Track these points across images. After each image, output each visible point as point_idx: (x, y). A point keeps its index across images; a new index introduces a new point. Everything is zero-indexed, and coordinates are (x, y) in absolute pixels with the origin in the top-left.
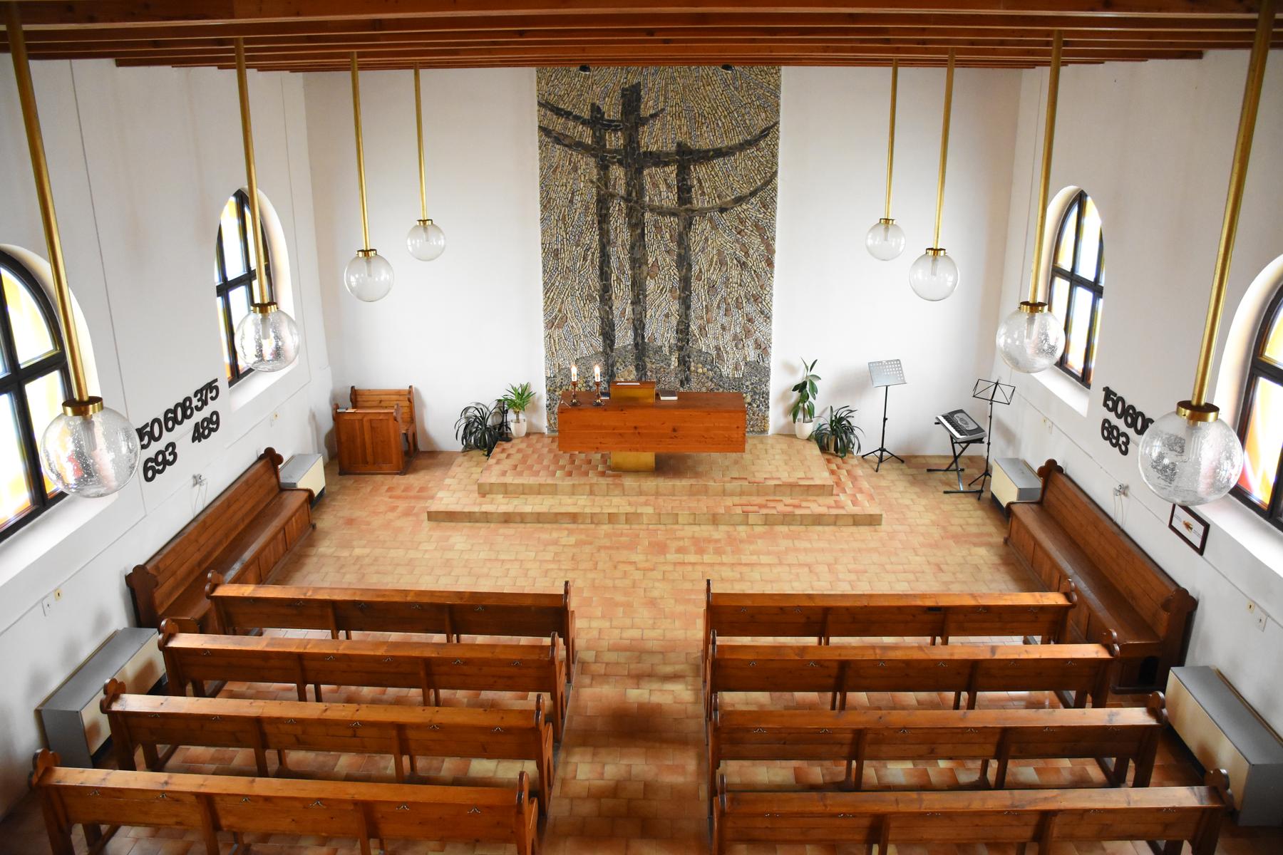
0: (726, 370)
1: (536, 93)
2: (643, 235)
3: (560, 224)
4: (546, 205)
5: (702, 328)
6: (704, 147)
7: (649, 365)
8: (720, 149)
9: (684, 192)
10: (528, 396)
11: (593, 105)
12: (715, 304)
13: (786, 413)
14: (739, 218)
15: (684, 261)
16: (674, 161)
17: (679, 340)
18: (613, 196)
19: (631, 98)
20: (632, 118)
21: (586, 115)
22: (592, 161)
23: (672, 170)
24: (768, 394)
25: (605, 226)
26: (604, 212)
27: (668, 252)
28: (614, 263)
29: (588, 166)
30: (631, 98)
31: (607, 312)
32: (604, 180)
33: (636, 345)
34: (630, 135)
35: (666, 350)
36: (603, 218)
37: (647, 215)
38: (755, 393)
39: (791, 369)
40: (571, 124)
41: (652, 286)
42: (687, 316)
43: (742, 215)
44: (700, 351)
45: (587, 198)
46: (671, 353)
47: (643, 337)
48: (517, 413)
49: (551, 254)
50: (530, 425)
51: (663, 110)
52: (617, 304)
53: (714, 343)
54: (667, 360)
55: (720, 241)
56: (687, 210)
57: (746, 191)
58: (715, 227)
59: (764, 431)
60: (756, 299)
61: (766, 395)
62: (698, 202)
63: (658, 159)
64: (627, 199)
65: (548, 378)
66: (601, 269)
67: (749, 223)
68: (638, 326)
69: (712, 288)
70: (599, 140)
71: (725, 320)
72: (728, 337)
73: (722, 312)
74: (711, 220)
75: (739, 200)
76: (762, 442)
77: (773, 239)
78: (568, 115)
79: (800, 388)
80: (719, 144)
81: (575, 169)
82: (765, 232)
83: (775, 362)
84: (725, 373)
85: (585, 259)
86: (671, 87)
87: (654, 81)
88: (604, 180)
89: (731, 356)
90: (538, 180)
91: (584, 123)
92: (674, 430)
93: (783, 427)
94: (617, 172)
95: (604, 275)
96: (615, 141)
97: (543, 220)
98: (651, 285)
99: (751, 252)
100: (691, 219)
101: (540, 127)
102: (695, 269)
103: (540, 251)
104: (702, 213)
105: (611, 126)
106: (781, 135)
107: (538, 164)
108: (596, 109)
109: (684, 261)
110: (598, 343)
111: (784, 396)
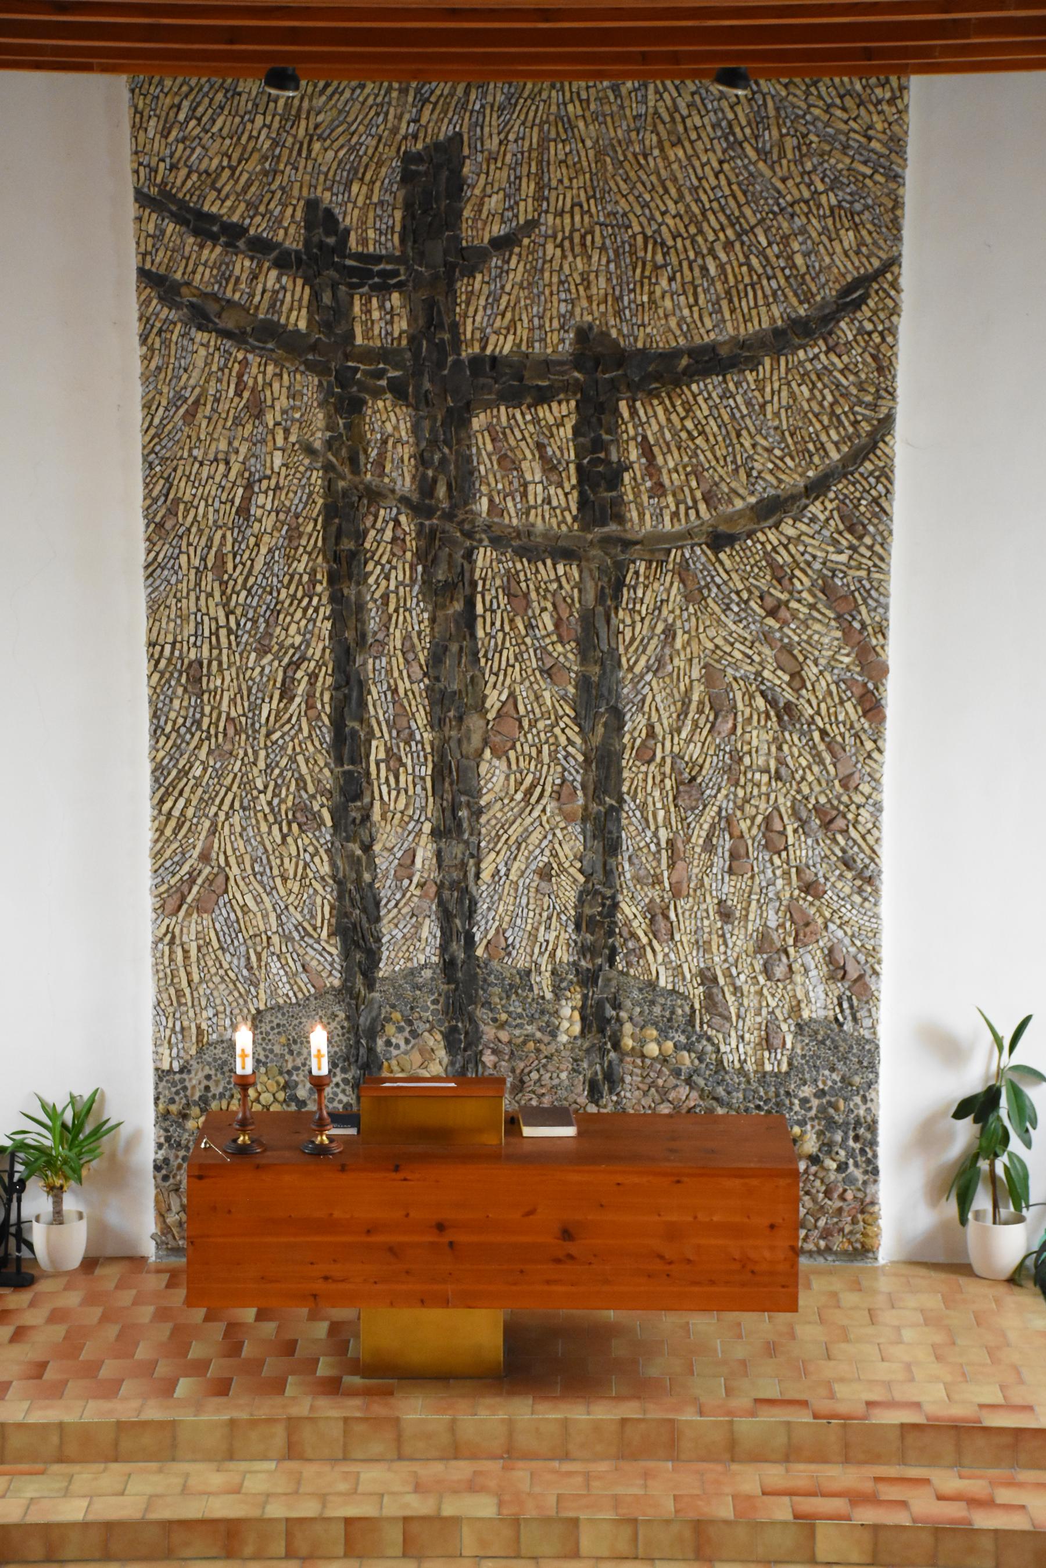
0: (737, 1049)
1: (128, 165)
2: (469, 618)
3: (209, 580)
4: (164, 519)
5: (655, 914)
6: (661, 344)
7: (489, 1032)
8: (712, 348)
9: (598, 484)
10: (98, 1132)
11: (312, 205)
12: (698, 838)
13: (937, 1191)
14: (772, 565)
15: (598, 701)
16: (569, 388)
17: (584, 950)
18: (374, 496)
19: (433, 184)
20: (436, 249)
21: (291, 237)
22: (309, 385)
23: (561, 415)
24: (872, 1127)
25: (350, 591)
26: (348, 545)
27: (548, 673)
28: (378, 705)
29: (295, 399)
30: (433, 184)
31: (355, 863)
32: (347, 447)
33: (448, 966)
34: (430, 305)
35: (543, 983)
36: (345, 566)
37: (484, 557)
38: (831, 1124)
39: (947, 1048)
40: (243, 265)
41: (497, 781)
42: (609, 874)
43: (783, 557)
44: (652, 985)
45: (294, 500)
46: (557, 991)
48: (56, 1192)
49: (179, 675)
50: (99, 1231)
51: (532, 224)
52: (387, 838)
53: (692, 963)
54: (545, 1015)
55: (711, 637)
56: (606, 541)
57: (794, 481)
58: (695, 595)
59: (864, 1251)
60: (828, 819)
61: (865, 1132)
62: (643, 518)
63: (518, 382)
64: (420, 506)
65: (161, 1075)
66: (338, 724)
67: (802, 582)
68: (455, 905)
69: (687, 785)
70: (333, 319)
71: (729, 888)
72: (740, 940)
73: (720, 863)
74: (683, 571)
75: (772, 509)
76: (857, 1286)
77: (881, 630)
78: (232, 234)
79: (979, 1107)
80: (708, 333)
81: (257, 410)
82: (855, 609)
83: (893, 1021)
84: (731, 1059)
85: (287, 693)
86: (556, 151)
87: (504, 129)
88: (347, 447)
89: (751, 1001)
90: (137, 442)
91: (284, 262)
92: (567, 1234)
93: (929, 1239)
94: (389, 422)
95: (347, 744)
96: (381, 321)
97: (152, 568)
98: (494, 776)
99: (811, 671)
100: (621, 567)
101: (144, 275)
102: (635, 725)
103: (144, 666)
104: (657, 549)
105: (370, 275)
106: (907, 300)
107: (137, 390)
108: (320, 219)
109: (598, 701)
110: (326, 960)
111: (926, 1136)
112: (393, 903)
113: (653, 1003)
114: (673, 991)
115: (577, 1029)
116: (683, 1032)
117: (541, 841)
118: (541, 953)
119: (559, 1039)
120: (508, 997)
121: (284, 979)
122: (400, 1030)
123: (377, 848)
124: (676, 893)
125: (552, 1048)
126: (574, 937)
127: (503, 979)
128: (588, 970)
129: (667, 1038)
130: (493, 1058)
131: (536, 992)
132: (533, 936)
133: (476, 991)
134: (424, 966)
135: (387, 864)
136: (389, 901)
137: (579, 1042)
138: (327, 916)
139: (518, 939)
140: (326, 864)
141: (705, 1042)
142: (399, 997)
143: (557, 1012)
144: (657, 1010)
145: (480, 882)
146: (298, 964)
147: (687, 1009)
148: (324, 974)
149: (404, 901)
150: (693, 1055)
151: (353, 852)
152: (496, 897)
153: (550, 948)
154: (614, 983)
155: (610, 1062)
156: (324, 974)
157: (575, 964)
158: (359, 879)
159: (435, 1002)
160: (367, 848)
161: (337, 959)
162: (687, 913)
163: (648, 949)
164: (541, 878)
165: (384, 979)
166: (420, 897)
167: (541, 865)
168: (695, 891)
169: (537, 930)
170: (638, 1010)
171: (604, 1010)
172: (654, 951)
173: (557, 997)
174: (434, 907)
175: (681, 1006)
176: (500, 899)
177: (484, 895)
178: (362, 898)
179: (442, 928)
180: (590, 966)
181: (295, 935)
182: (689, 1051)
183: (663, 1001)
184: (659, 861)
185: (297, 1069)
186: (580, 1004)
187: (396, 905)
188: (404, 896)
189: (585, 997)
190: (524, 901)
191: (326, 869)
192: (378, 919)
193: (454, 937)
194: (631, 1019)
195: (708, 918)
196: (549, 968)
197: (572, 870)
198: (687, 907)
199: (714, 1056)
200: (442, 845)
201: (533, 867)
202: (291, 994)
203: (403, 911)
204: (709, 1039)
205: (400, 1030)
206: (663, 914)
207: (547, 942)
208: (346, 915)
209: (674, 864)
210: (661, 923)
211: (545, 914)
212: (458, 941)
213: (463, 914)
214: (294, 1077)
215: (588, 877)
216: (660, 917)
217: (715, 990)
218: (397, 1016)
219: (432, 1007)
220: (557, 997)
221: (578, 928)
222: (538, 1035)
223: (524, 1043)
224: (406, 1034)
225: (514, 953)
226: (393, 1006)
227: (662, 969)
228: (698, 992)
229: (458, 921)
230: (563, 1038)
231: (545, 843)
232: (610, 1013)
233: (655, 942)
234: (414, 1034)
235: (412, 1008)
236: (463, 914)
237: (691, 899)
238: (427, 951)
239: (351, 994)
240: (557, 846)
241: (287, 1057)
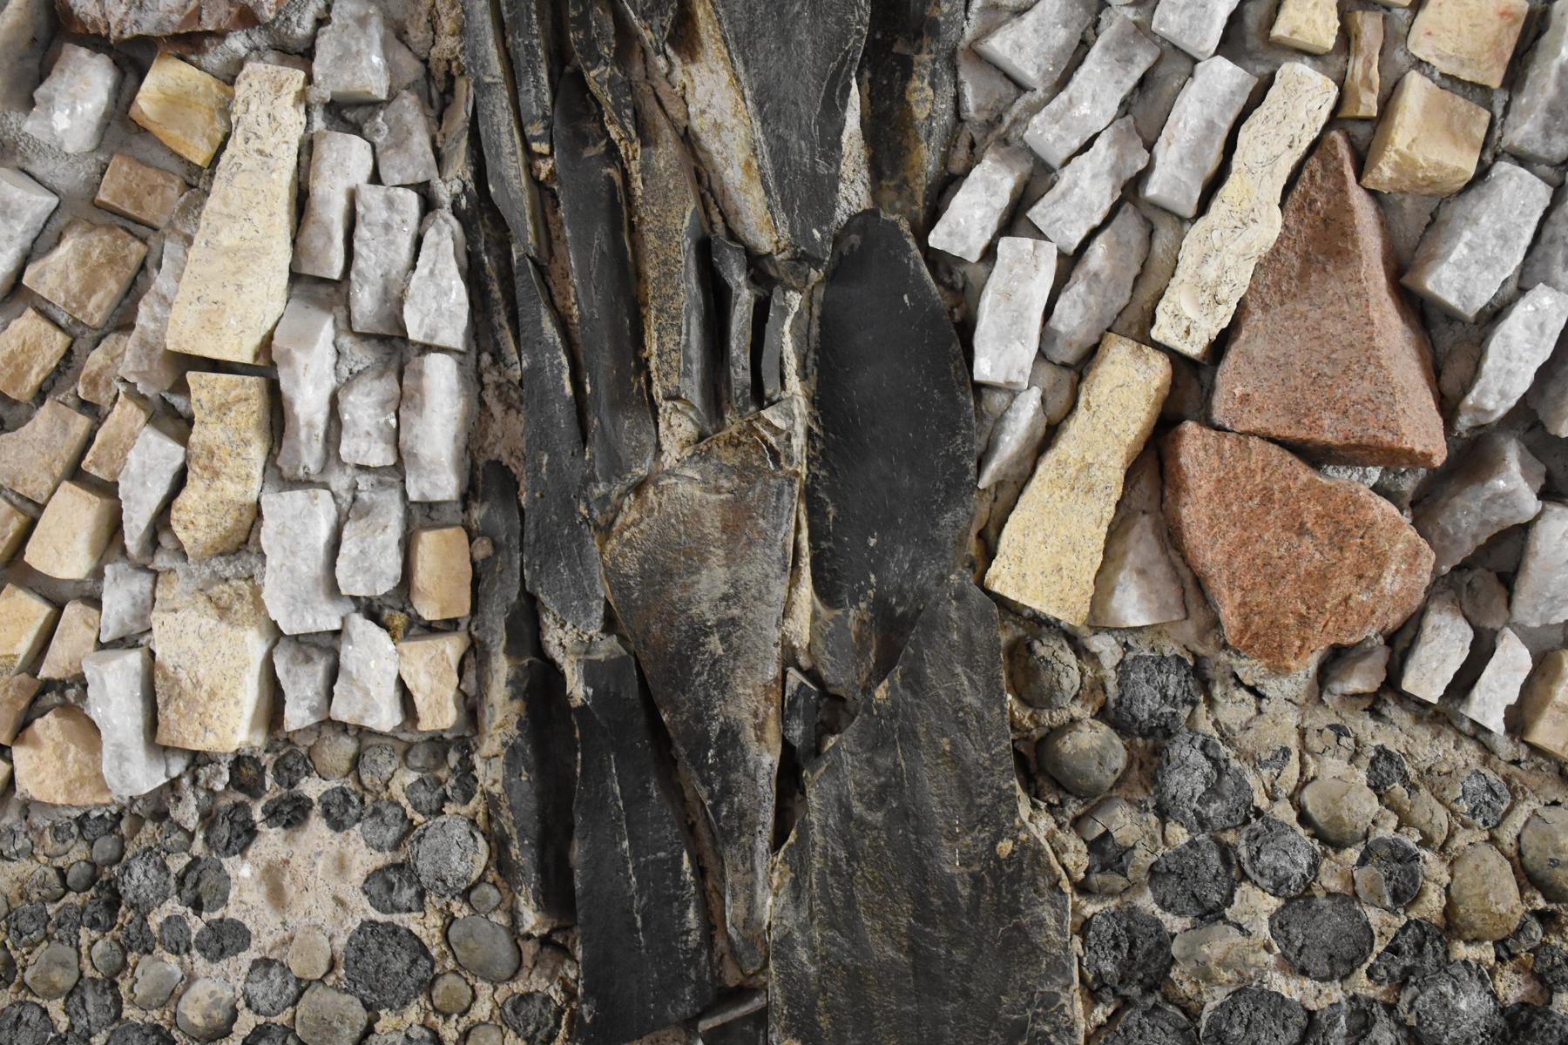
47: (898, 410)
134: (262, 788)
179: (481, 216)
193: (673, 343)
229: (713, 94)
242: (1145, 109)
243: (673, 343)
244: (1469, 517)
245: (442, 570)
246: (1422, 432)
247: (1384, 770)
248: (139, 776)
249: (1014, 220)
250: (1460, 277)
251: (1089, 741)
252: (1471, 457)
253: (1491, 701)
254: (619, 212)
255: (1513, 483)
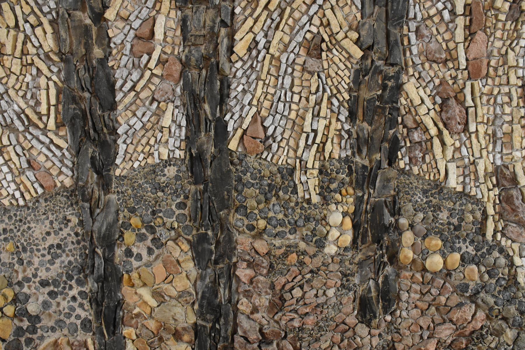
5: (447, 99)
7: (243, 241)
17: (360, 144)
33: (195, 161)
35: (309, 183)
44: (438, 187)
46: (325, 192)
47: (222, 134)
54: (311, 221)
68: (205, 89)
110: (54, 154)
112: (129, 85)
113: (438, 208)
114: (463, 194)
115: (348, 238)
116: (472, 242)
117: (309, 7)
118: (307, 147)
119: (326, 250)
120: (267, 201)
121: (9, 177)
122: (141, 238)
123: (110, 14)
124: (474, 72)
125: (318, 261)
126: (347, 127)
127: (262, 178)
128: (364, 167)
129: (453, 250)
130: (249, 272)
131: (301, 194)
132: (297, 126)
133: (229, 192)
134: (168, 163)
135: (122, 36)
136: (125, 82)
137: (350, 254)
138: (53, 101)
139: (279, 130)
140: (49, 35)
141: (496, 254)
142: (139, 199)
143: (324, 218)
144: (444, 216)
145: (234, 58)
146: (23, 159)
147: (479, 215)
148: (54, 172)
149: (142, 83)
150: (483, 269)
151: (81, 21)
152: (253, 77)
153: (318, 140)
154: (393, 183)
155: (386, 277)
156: (54, 172)
157: (347, 160)
158: (87, 57)
159: (182, 206)
160: (99, 17)
161: (67, 153)
162: (485, 98)
163: (436, 142)
164: (308, 54)
165: (121, 178)
166: (162, 77)
167: (309, 36)
168: (496, 69)
169: (303, 119)
170: (421, 215)
171: (382, 215)
172: (443, 144)
173: (326, 200)
174: (178, 90)
175: (472, 212)
176: (258, 79)
177: (239, 74)
178: (92, 79)
179: (187, 116)
180: (366, 163)
181: (17, 123)
182: (477, 264)
183: (450, 205)
184: (453, 34)
185: (28, 280)
186: (352, 209)
187: (133, 88)
188: (142, 76)
189: (359, 201)
190: (288, 81)
191: (49, 43)
192: (113, 106)
193: (203, 127)
194: (412, 226)
195: (509, 104)
196: (317, 165)
197: (346, 43)
198: (485, 90)
199: (506, 270)
200: (188, 12)
201: (299, 38)
202: (17, 194)
203: (143, 95)
204: (502, 251)
205: (141, 238)
206: (456, 97)
207: (315, 131)
208: (74, 100)
209: (472, 34)
210: (456, 110)
211: (313, 98)
212: (207, 131)
213: (213, 97)
214: (26, 290)
215: (367, 49)
216: (452, 102)
217: (514, 192)
218: (135, 221)
219: (177, 212)
220: (326, 200)
221: (352, 116)
222: (302, 245)
223: (286, 255)
224: (149, 243)
225: (275, 146)
226: (133, 211)
227: (452, 167)
228: (488, 194)
229: (207, 107)
230: (331, 249)
231: (314, 8)
232: (389, 219)
233: (446, 132)
234: (158, 243)
235: (154, 213)
236: (213, 97)
237: (490, 81)
238: (171, 145)
239: (83, 195)
240: (328, 13)
241: (16, 266)
242: (242, 109)
243: (203, 127)
244: (267, 144)
245: (183, 144)
246: (262, 135)
247: (260, 164)
248: (158, 161)
249: (231, 118)
250: (266, 124)
251: (236, 160)
252: (267, 138)
253: (269, 159)
254: (199, 116)
255: (270, 141)
